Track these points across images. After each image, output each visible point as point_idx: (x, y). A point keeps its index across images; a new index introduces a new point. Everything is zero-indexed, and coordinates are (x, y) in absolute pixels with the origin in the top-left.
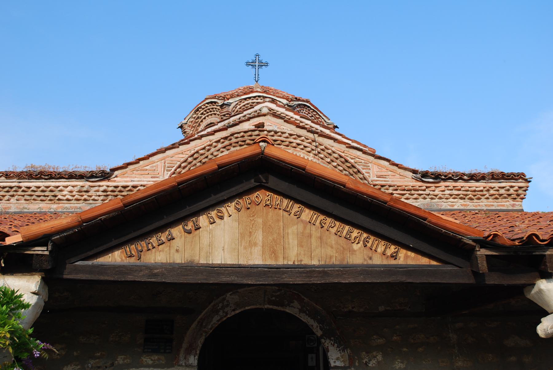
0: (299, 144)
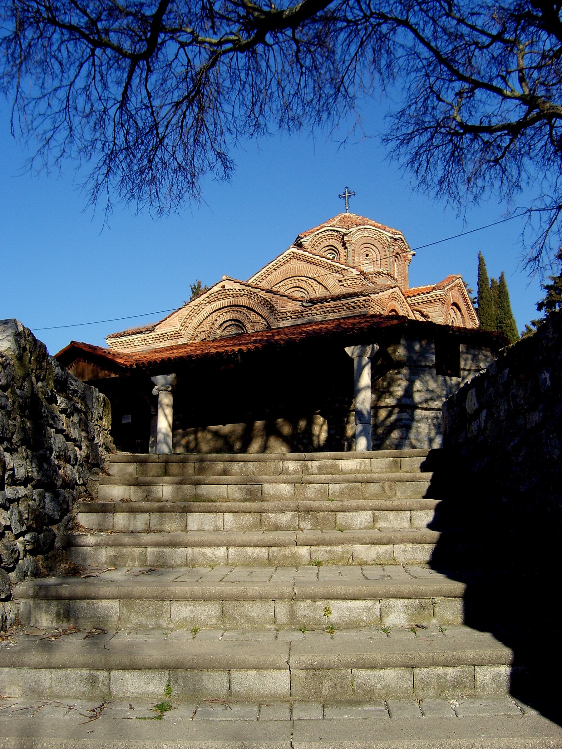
0: (244, 295)
